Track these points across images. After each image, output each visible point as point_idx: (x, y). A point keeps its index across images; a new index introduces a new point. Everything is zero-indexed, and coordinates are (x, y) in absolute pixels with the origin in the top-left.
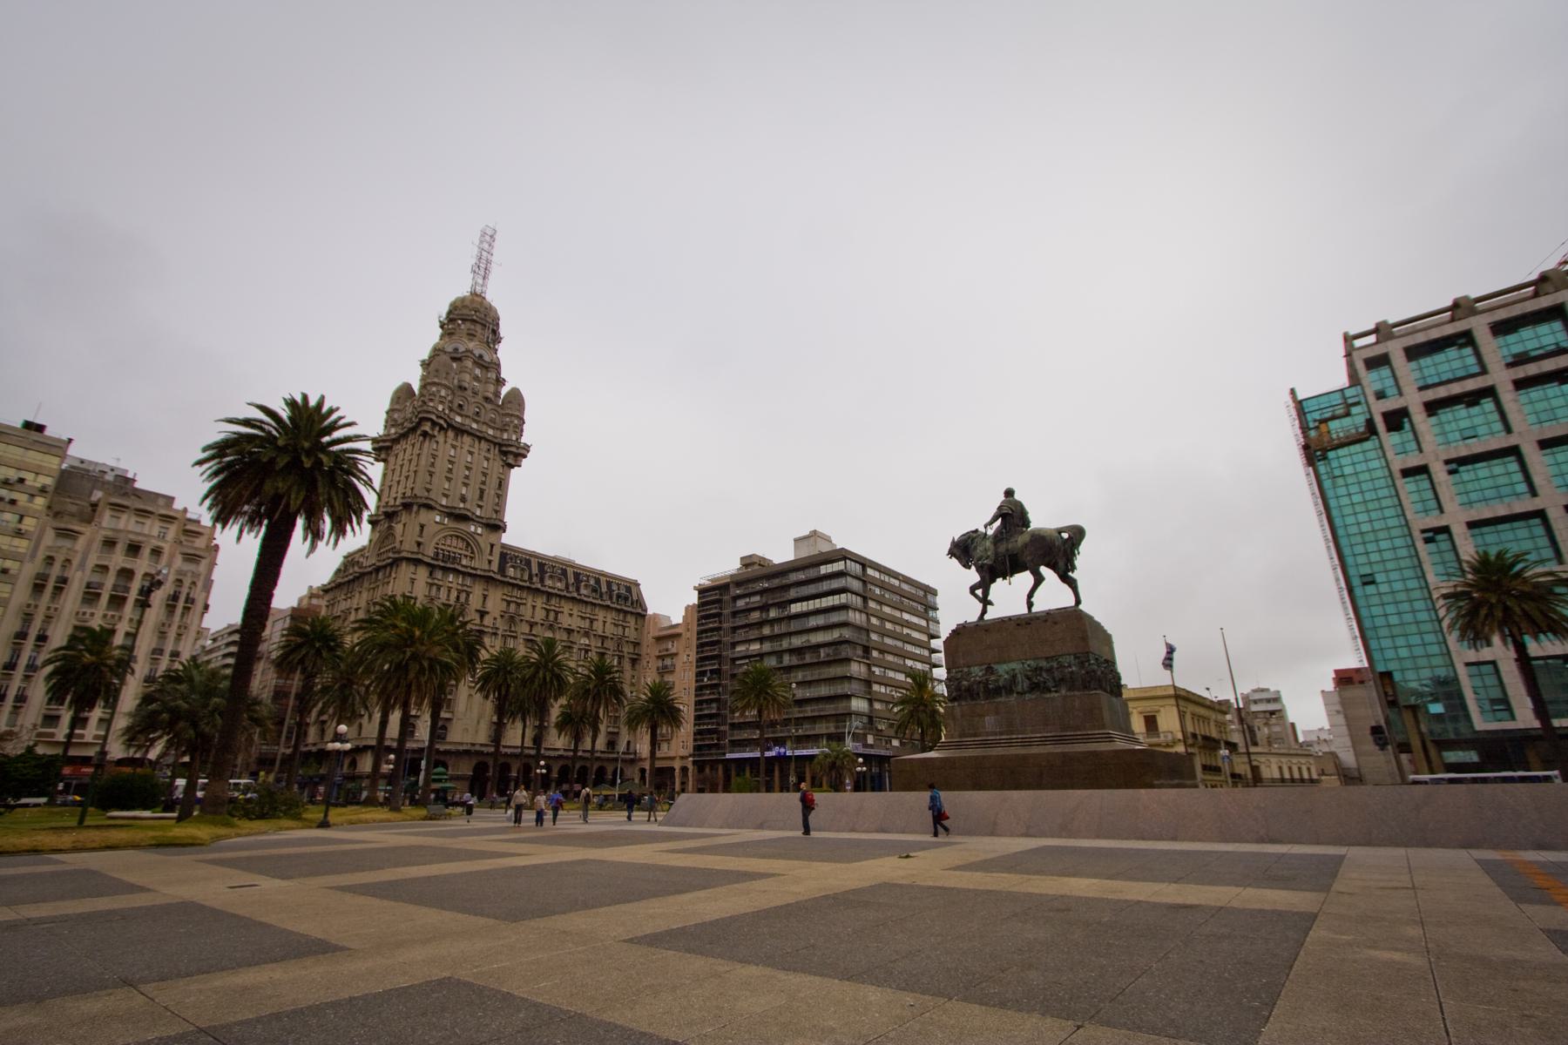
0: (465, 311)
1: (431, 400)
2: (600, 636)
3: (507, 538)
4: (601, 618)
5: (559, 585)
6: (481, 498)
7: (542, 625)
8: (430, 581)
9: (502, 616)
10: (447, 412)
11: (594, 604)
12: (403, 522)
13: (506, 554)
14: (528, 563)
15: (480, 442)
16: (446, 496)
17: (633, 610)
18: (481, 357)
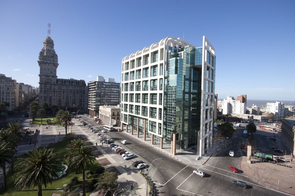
3: (57, 78)
5: (68, 84)
6: (51, 73)
18: (49, 49)
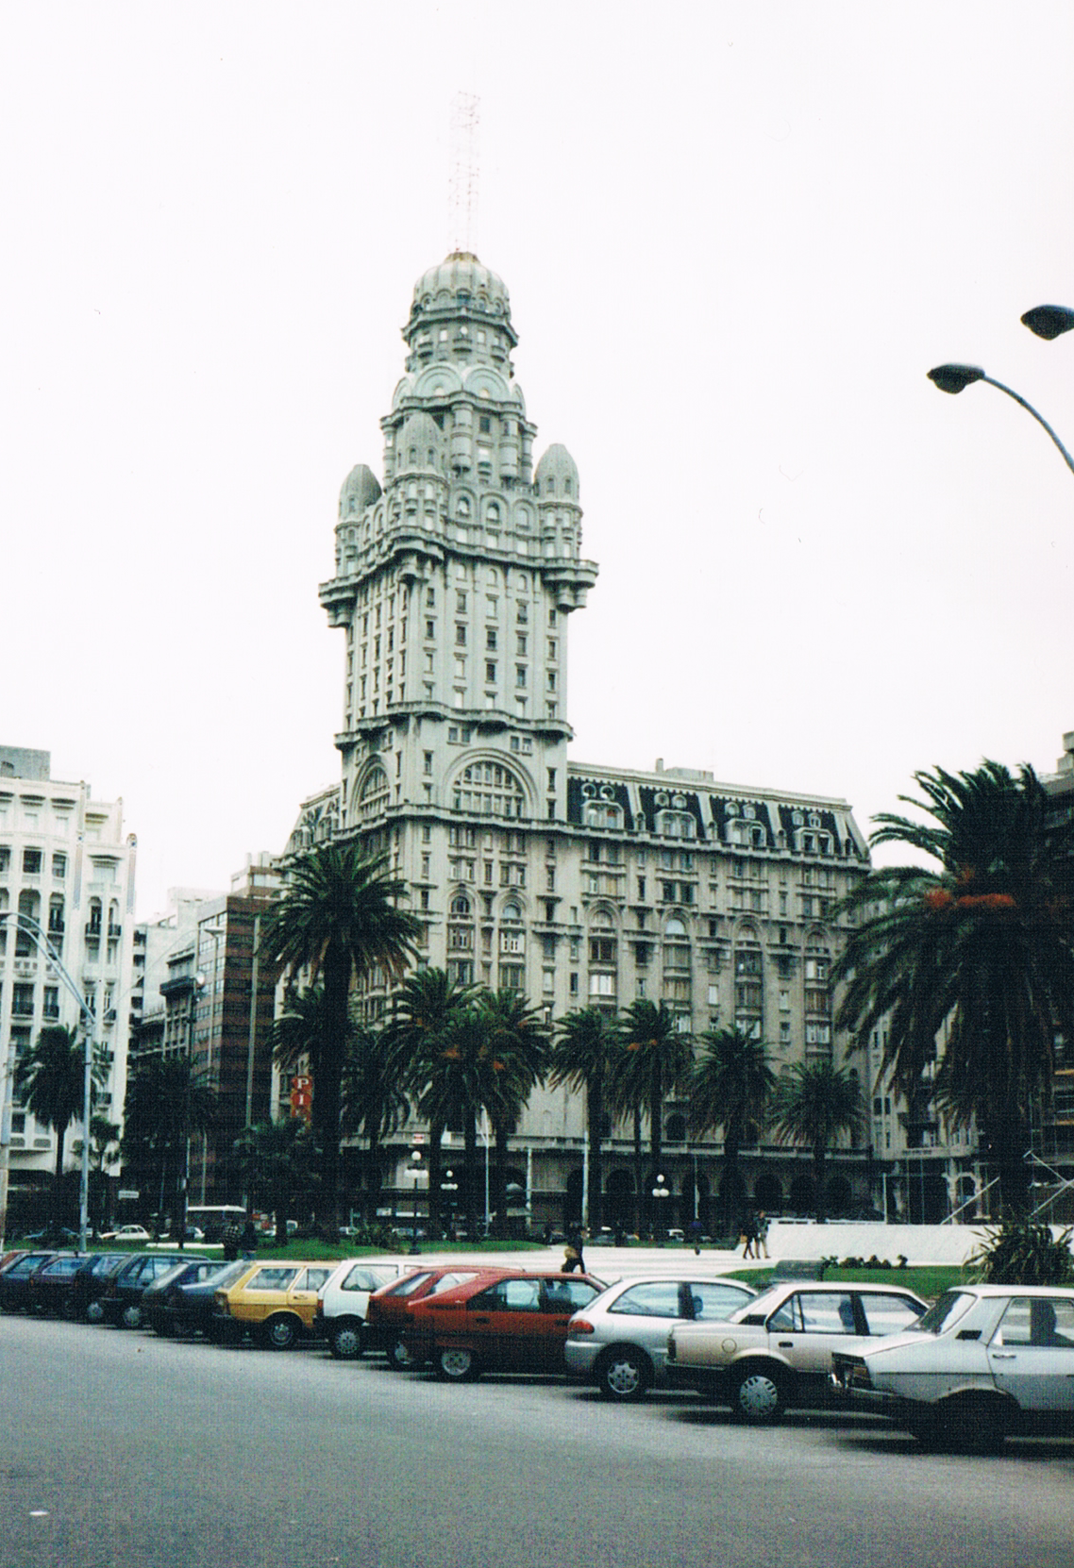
0: (441, 304)
1: (411, 512)
2: (777, 923)
4: (774, 885)
7: (661, 912)
8: (454, 852)
9: (585, 903)
10: (440, 529)
11: (759, 861)
12: (395, 750)
13: (580, 782)
14: (621, 794)
15: (506, 574)
16: (460, 690)
17: (841, 864)
